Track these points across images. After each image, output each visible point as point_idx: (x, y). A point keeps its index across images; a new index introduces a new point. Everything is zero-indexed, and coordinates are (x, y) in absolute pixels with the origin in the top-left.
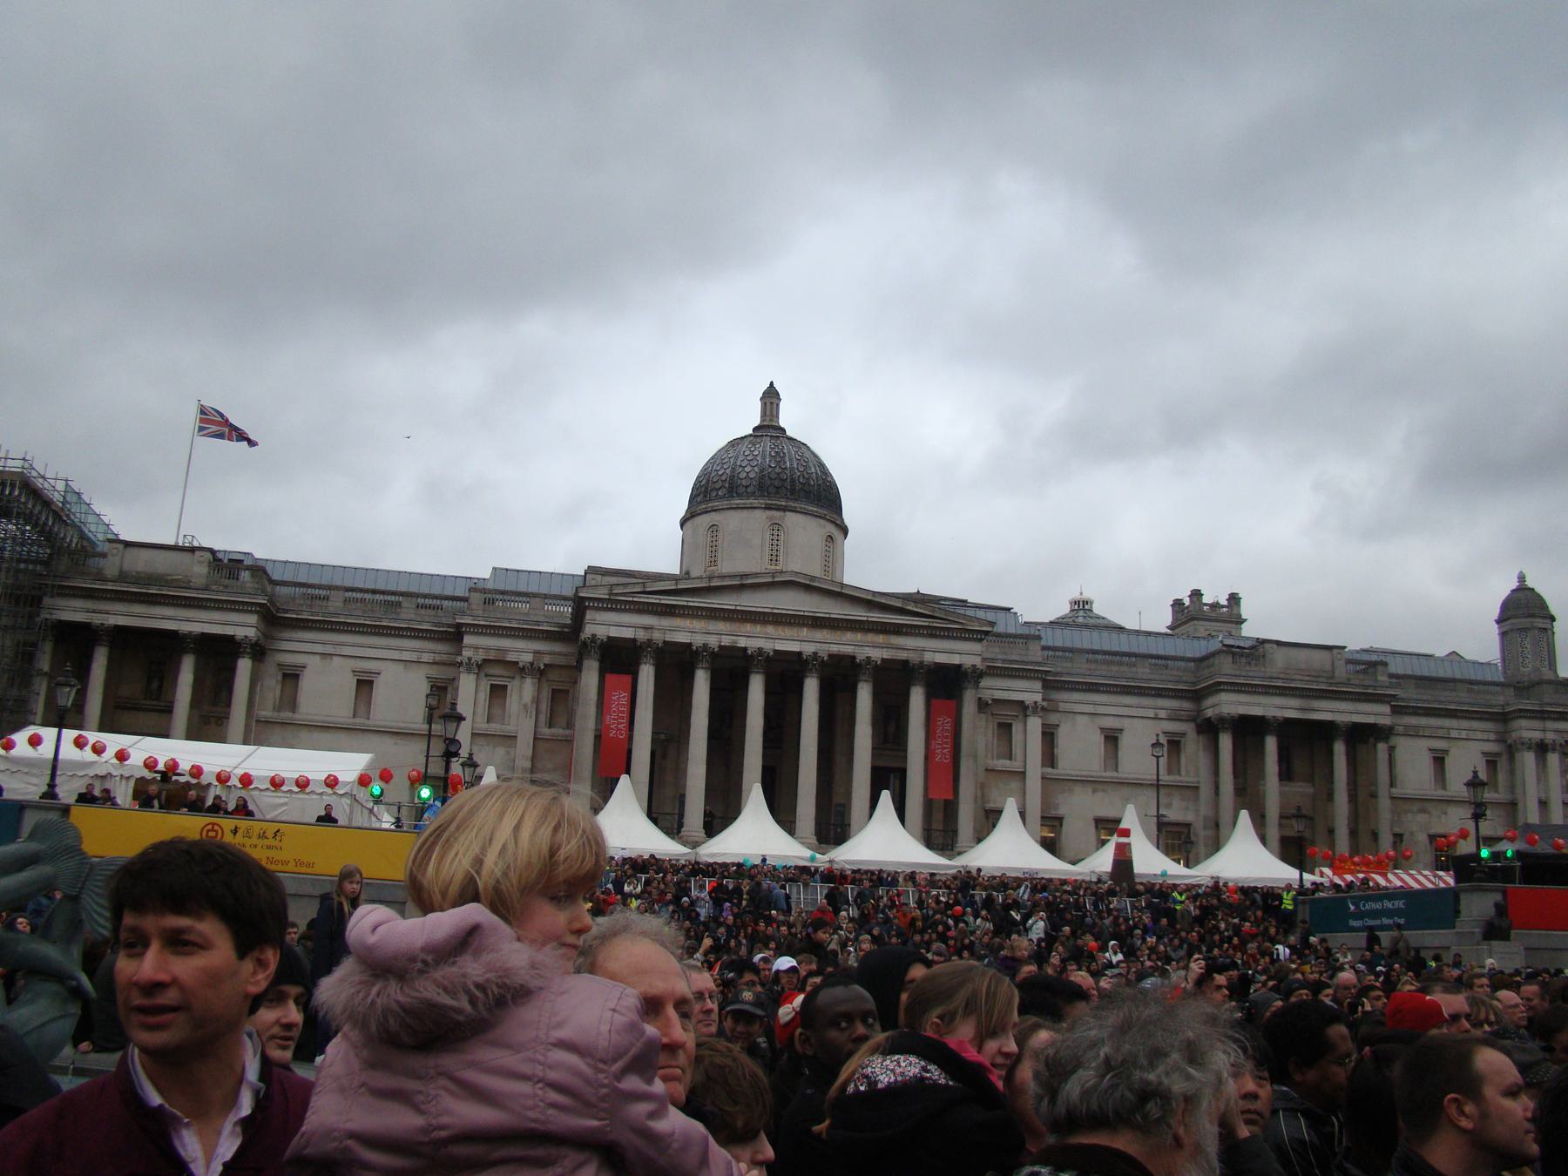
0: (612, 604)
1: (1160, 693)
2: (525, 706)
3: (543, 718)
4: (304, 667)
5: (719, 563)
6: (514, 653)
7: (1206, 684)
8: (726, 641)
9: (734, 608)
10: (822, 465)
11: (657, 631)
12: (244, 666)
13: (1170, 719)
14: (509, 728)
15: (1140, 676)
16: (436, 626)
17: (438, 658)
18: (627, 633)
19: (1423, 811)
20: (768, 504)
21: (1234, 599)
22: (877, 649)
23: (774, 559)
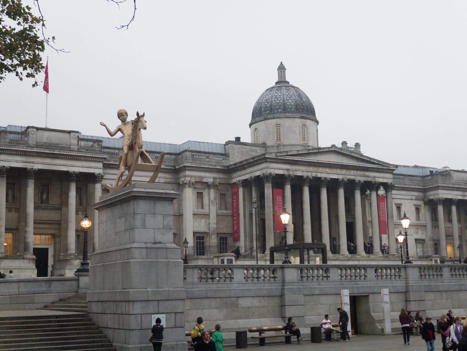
0: (276, 160)
2: (212, 201)
5: (282, 140)
6: (206, 178)
7: (432, 186)
8: (314, 175)
9: (317, 161)
10: (307, 98)
11: (291, 171)
13: (416, 200)
14: (206, 210)
15: (406, 183)
16: (166, 166)
17: (167, 180)
18: (281, 172)
20: (301, 116)
21: (357, 145)
22: (361, 177)
23: (304, 139)
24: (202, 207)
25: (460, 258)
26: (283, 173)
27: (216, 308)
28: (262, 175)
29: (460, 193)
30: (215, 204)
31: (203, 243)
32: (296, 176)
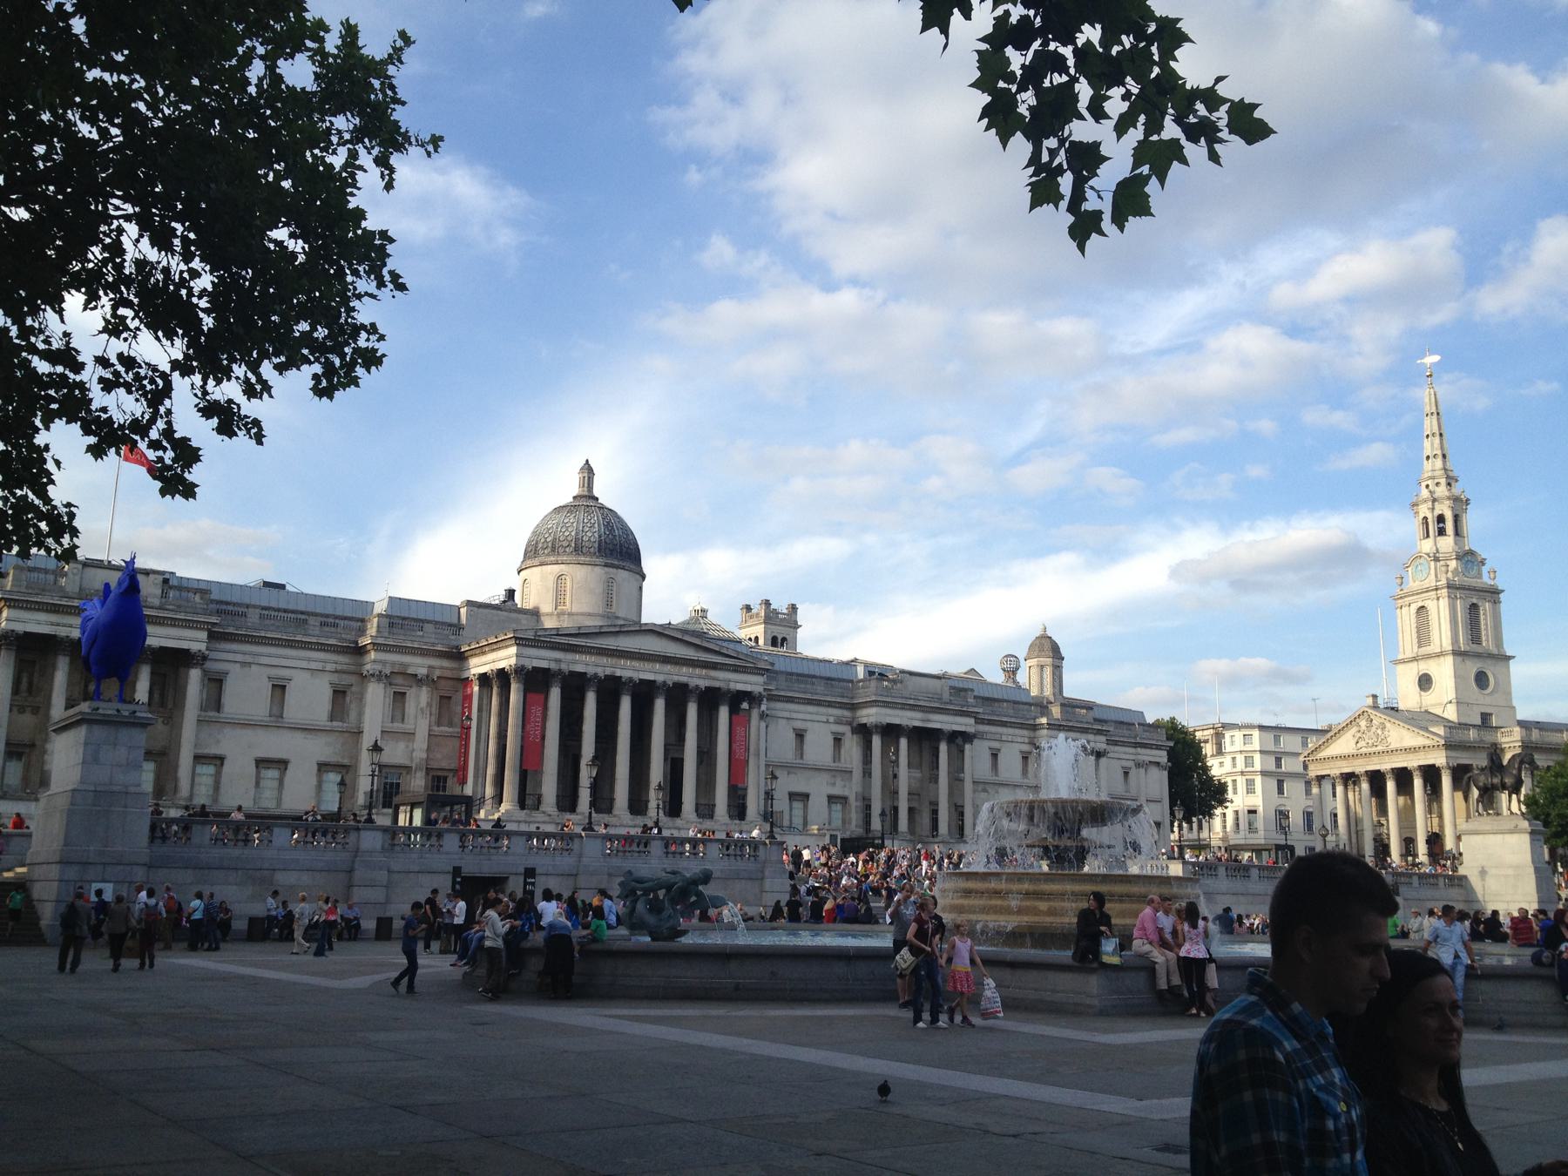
1: (830, 704)
2: (422, 709)
3: (433, 718)
4: (227, 674)
8: (608, 671)
12: (195, 675)
13: (836, 723)
14: (408, 726)
17: (339, 668)
18: (544, 664)
19: (985, 790)
21: (793, 608)
23: (609, 604)
24: (403, 720)
25: (883, 834)
26: (547, 667)
27: (236, 884)
28: (508, 667)
29: (919, 715)
30: (428, 713)
31: (398, 784)
32: (572, 673)
